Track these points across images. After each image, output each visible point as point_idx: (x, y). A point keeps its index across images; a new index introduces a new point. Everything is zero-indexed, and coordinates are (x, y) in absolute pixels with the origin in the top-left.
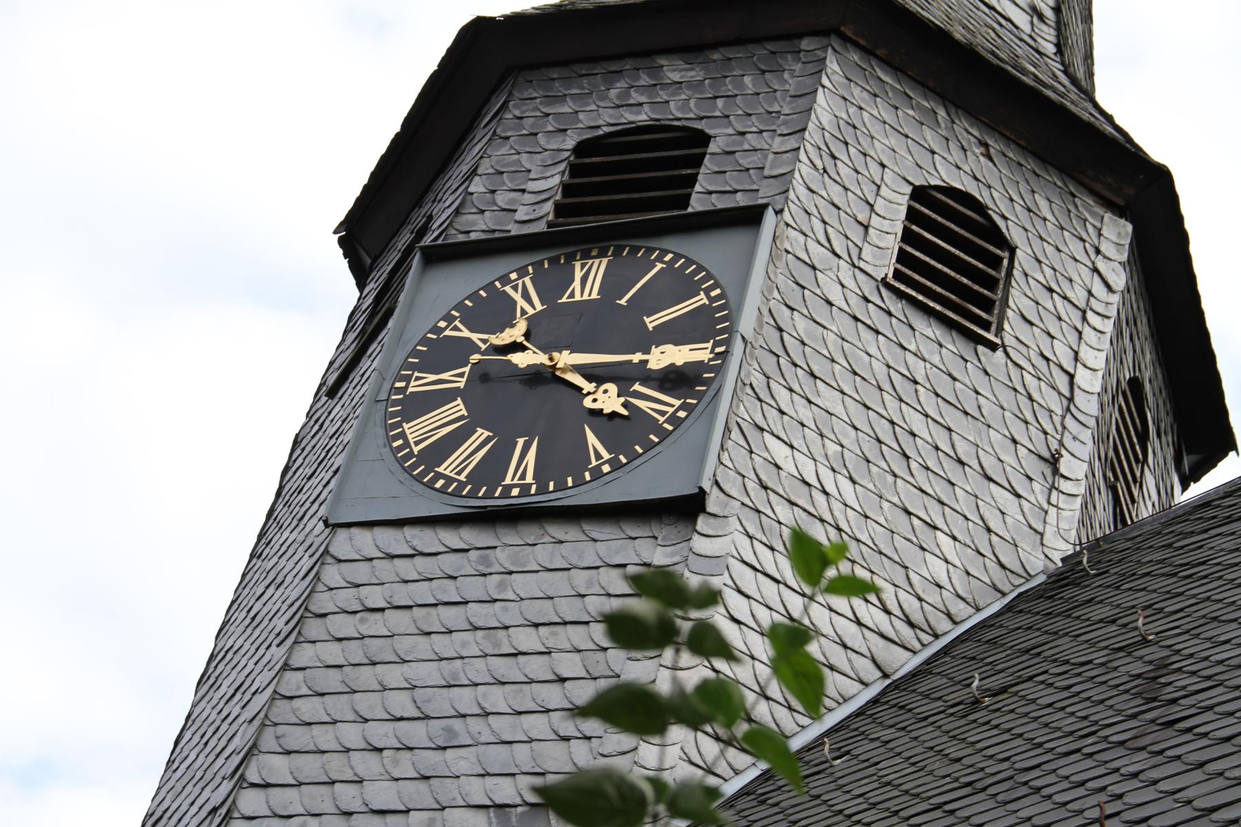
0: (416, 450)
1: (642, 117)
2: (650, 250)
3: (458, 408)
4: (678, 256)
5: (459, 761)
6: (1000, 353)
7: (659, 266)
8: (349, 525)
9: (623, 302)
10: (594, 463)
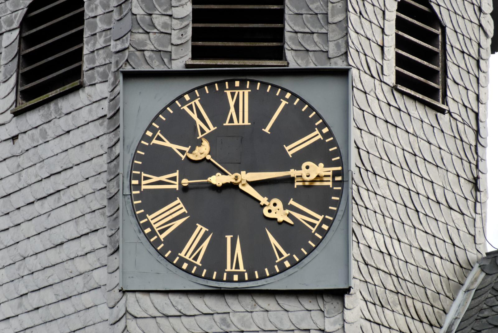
2: (275, 87)
7: (284, 103)
9: (267, 130)
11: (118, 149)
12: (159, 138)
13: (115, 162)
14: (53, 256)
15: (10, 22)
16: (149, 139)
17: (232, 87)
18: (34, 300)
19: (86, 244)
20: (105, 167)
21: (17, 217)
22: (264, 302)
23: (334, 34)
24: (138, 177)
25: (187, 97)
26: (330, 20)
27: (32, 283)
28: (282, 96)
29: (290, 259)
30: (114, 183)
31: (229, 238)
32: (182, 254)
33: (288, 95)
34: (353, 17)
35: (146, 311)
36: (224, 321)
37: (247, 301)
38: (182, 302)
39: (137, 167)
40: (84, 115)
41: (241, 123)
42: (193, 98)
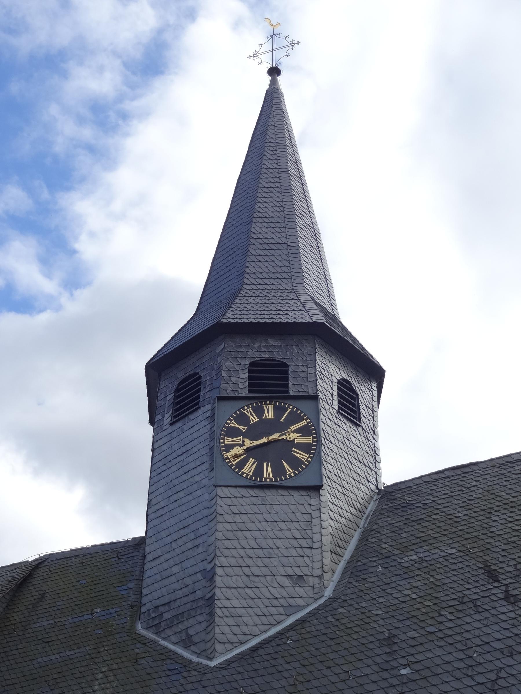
1: (267, 356)
2: (285, 404)
4: (294, 407)
5: (275, 561)
7: (289, 410)
8: (221, 486)
9: (282, 420)
10: (288, 473)
11: (215, 428)
12: (233, 423)
13: (213, 434)
14: (184, 477)
15: (171, 391)
16: (229, 424)
17: (266, 404)
18: (175, 497)
19: (199, 469)
20: (209, 437)
21: (169, 465)
22: (282, 492)
23: (311, 385)
24: (223, 439)
25: (246, 408)
26: (309, 380)
27: (174, 490)
28: (289, 407)
29: (294, 473)
30: (212, 442)
31: (265, 464)
32: (243, 470)
33: (291, 407)
34: (319, 380)
35: (226, 495)
36: (263, 499)
37: (274, 492)
38: (244, 492)
39: (223, 435)
40: (200, 418)
41: (270, 418)
42: (248, 408)
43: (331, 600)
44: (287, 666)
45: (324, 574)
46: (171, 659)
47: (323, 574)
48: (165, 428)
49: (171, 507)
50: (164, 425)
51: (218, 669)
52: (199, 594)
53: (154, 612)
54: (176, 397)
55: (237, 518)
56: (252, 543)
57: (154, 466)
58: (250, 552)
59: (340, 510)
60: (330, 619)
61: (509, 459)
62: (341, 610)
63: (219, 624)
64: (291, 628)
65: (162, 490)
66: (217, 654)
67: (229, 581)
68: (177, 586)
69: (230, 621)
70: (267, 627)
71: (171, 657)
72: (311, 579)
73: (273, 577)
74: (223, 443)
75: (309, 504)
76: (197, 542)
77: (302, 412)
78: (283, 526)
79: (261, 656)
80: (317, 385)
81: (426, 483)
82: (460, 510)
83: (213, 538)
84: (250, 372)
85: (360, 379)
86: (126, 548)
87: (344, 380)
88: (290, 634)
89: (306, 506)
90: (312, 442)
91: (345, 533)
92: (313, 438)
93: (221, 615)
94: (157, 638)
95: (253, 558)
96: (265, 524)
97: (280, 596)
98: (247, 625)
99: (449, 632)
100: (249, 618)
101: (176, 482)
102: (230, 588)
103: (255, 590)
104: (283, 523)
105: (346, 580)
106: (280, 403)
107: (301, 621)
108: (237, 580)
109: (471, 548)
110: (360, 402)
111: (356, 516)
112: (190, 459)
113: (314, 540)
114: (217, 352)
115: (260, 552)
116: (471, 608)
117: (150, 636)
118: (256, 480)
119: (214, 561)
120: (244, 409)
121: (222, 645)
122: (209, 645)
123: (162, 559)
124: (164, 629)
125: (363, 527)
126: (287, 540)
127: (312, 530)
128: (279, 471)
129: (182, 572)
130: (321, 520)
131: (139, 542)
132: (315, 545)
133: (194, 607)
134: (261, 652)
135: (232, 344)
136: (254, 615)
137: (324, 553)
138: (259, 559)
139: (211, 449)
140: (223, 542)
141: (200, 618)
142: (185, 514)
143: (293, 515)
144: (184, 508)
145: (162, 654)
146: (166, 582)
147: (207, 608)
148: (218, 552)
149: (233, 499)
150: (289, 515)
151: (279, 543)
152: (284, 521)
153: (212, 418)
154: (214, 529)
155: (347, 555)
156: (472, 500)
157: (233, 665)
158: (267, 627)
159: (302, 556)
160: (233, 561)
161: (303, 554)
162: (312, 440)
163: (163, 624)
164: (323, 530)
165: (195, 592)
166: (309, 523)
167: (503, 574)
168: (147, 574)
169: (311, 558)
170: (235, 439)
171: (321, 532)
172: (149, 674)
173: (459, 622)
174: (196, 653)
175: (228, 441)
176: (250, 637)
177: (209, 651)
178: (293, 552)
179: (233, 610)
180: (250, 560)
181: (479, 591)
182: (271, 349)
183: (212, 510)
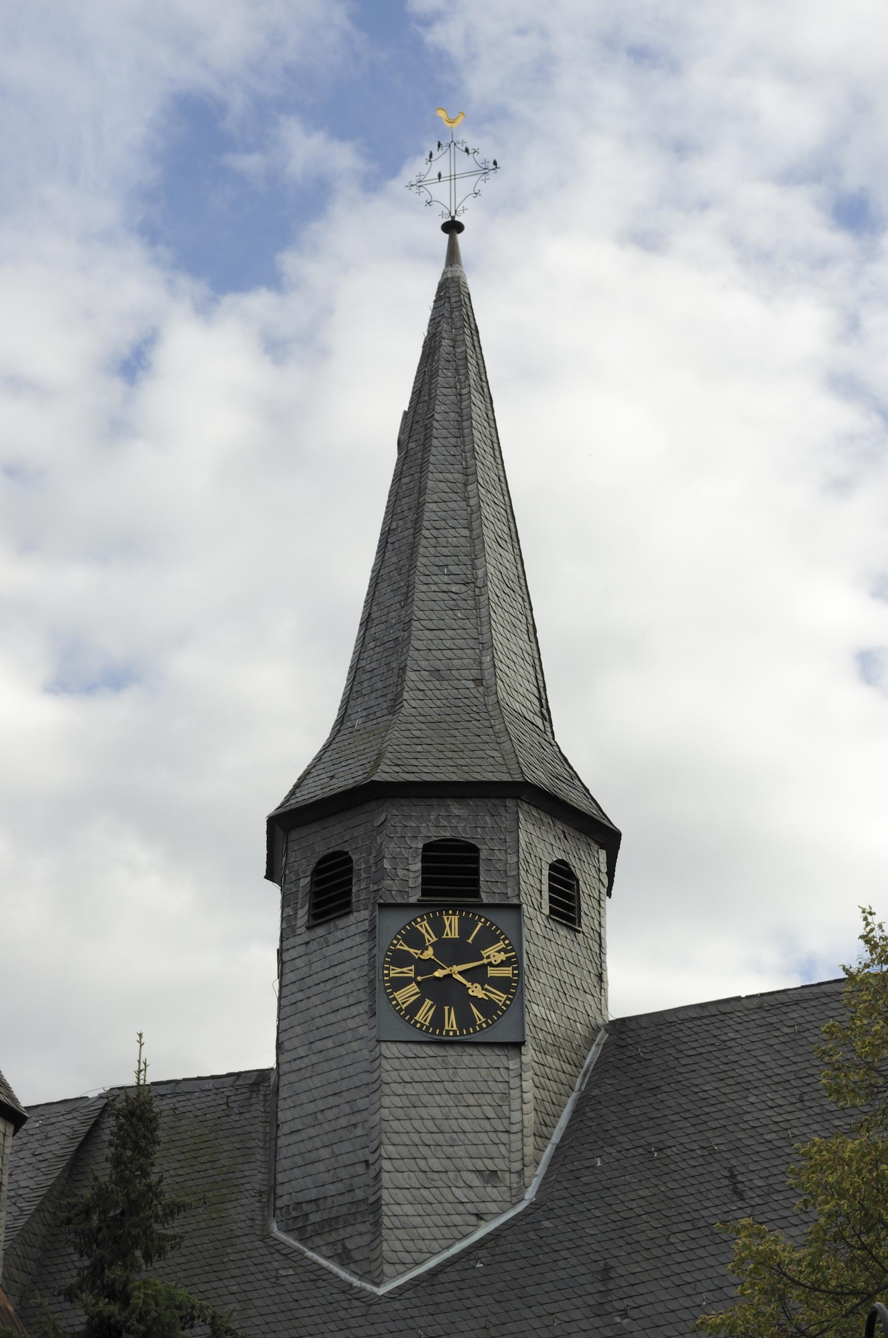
0: (404, 1007)
1: (448, 834)
2: (474, 915)
3: (413, 988)
4: (487, 920)
5: (460, 1151)
6: (582, 934)
7: (480, 925)
9: (470, 941)
11: (375, 951)
12: (401, 945)
13: (373, 959)
15: (305, 872)
16: (395, 945)
17: (447, 914)
18: (319, 1045)
19: (354, 1011)
20: (367, 962)
21: (309, 993)
22: (469, 1050)
24: (388, 969)
25: (419, 920)
26: (508, 874)
28: (479, 920)
29: (486, 1022)
31: (446, 1008)
32: (416, 1018)
33: (483, 920)
34: (522, 873)
35: (393, 1054)
36: (444, 1060)
37: (459, 1049)
38: (417, 1049)
39: (387, 963)
40: (353, 930)
41: (453, 936)
42: (423, 920)
43: (533, 1206)
44: (476, 1301)
45: (525, 1169)
46: (324, 1280)
47: (523, 1169)
48: (298, 931)
49: (314, 1059)
50: (298, 926)
51: (389, 1300)
52: (359, 1194)
53: (294, 1209)
54: (314, 883)
55: (409, 1089)
56: (430, 1125)
57: (284, 989)
58: (427, 1138)
59: (548, 1070)
60: (532, 1235)
61: (783, 998)
62: (546, 1224)
63: (386, 1238)
64: (480, 1244)
65: (298, 1030)
66: (385, 1279)
67: (400, 1179)
68: (327, 1178)
69: (400, 1233)
70: (450, 1242)
71: (324, 1277)
72: (507, 1175)
73: (458, 1173)
74: (388, 975)
75: (506, 1068)
76: (354, 1119)
77: (497, 929)
78: (471, 1100)
79: (443, 1283)
80: (519, 883)
81: (668, 1025)
82: (709, 1079)
83: (376, 1118)
84: (423, 861)
85: (582, 853)
86: (237, 1089)
87: (559, 861)
88: (481, 1253)
89: (502, 1070)
90: (511, 975)
91: (554, 1104)
92: (514, 969)
93: (390, 1226)
94: (301, 1247)
95: (432, 1147)
96: (446, 1097)
97: (466, 1200)
98: (424, 1239)
99: (677, 1269)
100: (426, 1230)
101: (319, 1022)
102: (401, 1188)
103: (434, 1191)
104: (471, 1095)
105: (553, 1178)
106: (468, 913)
107: (494, 1236)
108: (409, 1178)
109: (716, 1145)
110: (581, 892)
111: (570, 1075)
112: (341, 991)
113: (513, 1121)
114: (376, 825)
115: (439, 1138)
116: (708, 1236)
117: (292, 1243)
118: (434, 1032)
119: (379, 1150)
120: (417, 923)
121: (391, 1266)
122: (374, 1266)
123: (304, 1135)
124: (311, 1236)
125: (579, 1090)
126: (476, 1121)
127: (509, 1105)
128: (465, 1020)
129: (333, 1159)
130: (522, 1092)
131: (256, 1080)
132: (514, 1128)
133: (352, 1211)
134: (443, 1278)
135: (397, 813)
136: (433, 1225)
137: (525, 1139)
138: (439, 1148)
139: (371, 982)
140: (391, 1123)
141: (361, 1228)
142: (335, 1075)
143: (485, 1084)
144: (333, 1064)
145: (311, 1272)
146: (311, 1169)
147: (371, 1216)
148: (385, 1139)
149: (404, 1061)
150: (480, 1084)
151: (466, 1125)
152: (472, 1094)
153: (371, 933)
154: (377, 1105)
155: (556, 1136)
156: (727, 1064)
157: (407, 1295)
158: (450, 1242)
159: (497, 1144)
160: (404, 1151)
161: (497, 1141)
162: (511, 972)
163: (309, 1228)
164: (524, 1106)
165: (353, 1190)
166: (506, 1096)
167: (751, 1189)
168: (282, 1153)
169: (508, 1146)
170: (404, 970)
171: (522, 1109)
172: (297, 1301)
173: (690, 1255)
174: (357, 1274)
175: (395, 972)
176: (428, 1255)
177: (377, 1273)
178: (484, 1138)
179: (404, 1219)
180: (427, 1148)
181: (719, 1212)
182: (454, 822)
183: (375, 1076)
